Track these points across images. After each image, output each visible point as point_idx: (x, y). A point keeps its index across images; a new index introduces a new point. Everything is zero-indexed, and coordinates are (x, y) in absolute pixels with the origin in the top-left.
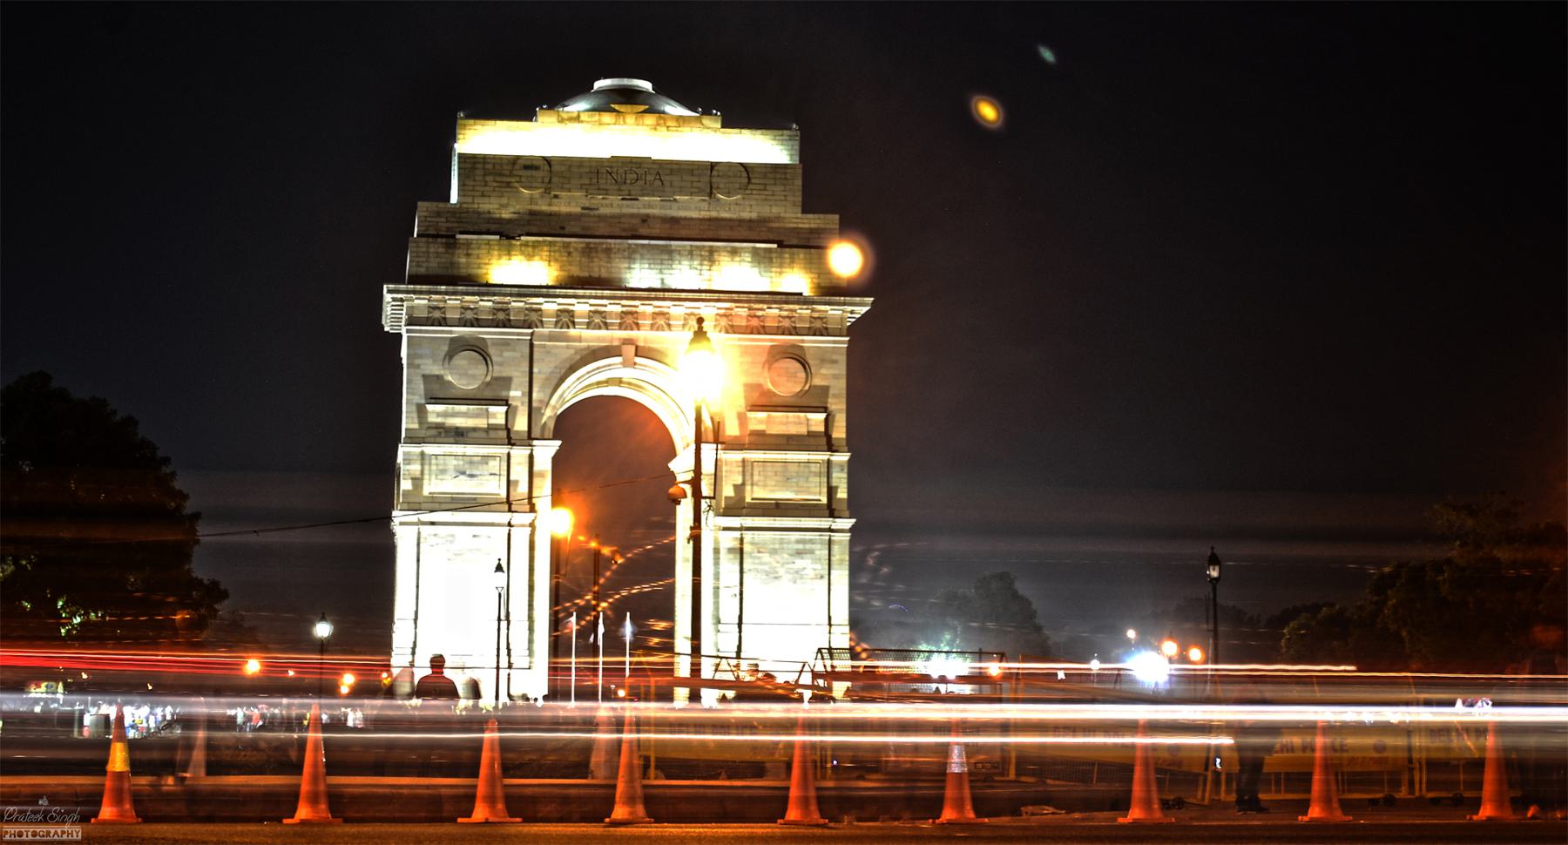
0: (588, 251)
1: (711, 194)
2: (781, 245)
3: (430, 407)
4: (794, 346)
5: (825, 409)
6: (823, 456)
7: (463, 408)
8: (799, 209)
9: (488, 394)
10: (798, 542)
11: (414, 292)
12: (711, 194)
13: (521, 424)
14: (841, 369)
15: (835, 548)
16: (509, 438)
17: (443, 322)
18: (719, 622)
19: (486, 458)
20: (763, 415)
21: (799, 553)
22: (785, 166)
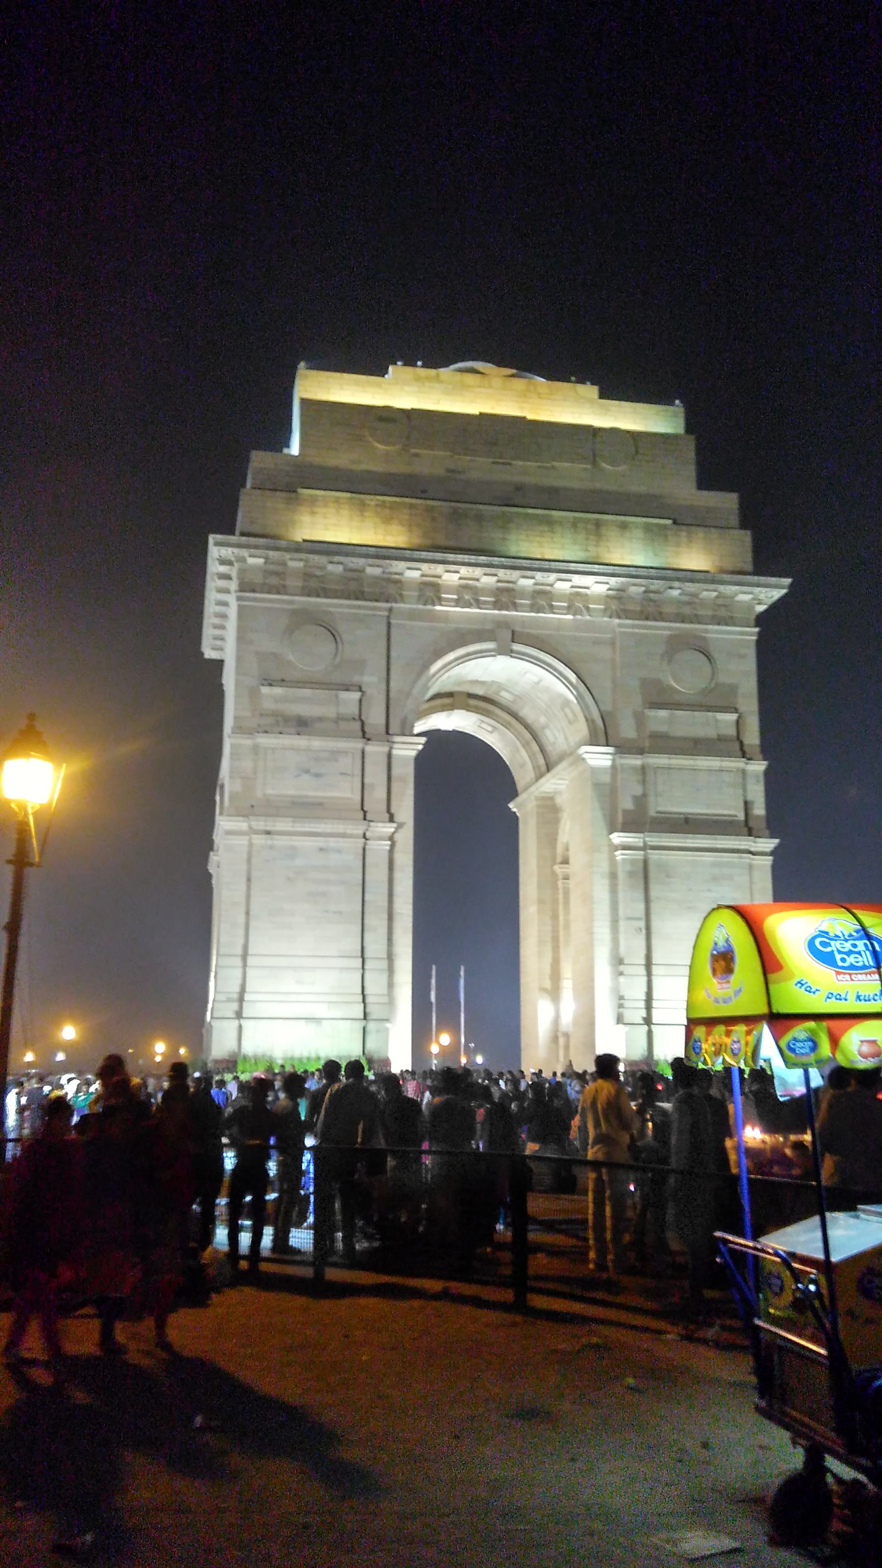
0: (456, 517)
1: (594, 463)
2: (675, 523)
3: (265, 690)
4: (696, 637)
5: (736, 710)
6: (739, 764)
7: (307, 692)
8: (694, 484)
9: (338, 677)
10: (714, 865)
11: (247, 546)
12: (594, 463)
13: (375, 717)
14: (750, 665)
15: (756, 874)
16: (364, 732)
17: (280, 590)
18: (621, 962)
19: (335, 755)
20: (663, 713)
21: (715, 879)
22: (675, 437)
